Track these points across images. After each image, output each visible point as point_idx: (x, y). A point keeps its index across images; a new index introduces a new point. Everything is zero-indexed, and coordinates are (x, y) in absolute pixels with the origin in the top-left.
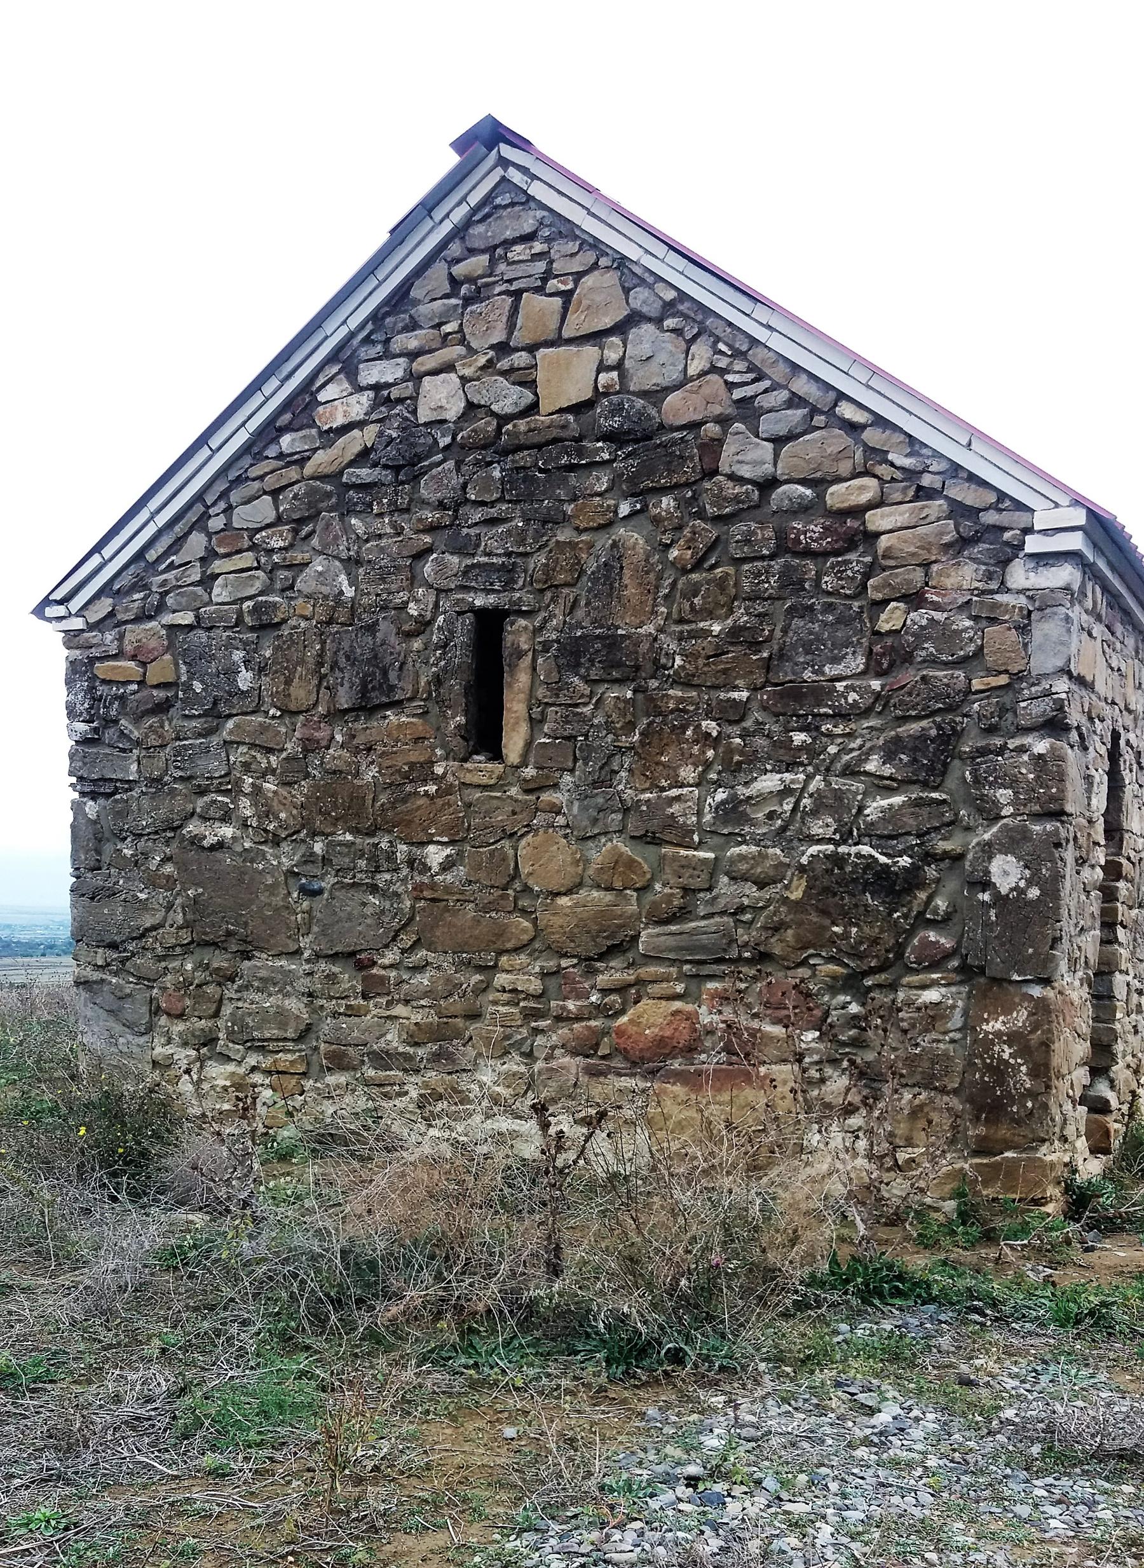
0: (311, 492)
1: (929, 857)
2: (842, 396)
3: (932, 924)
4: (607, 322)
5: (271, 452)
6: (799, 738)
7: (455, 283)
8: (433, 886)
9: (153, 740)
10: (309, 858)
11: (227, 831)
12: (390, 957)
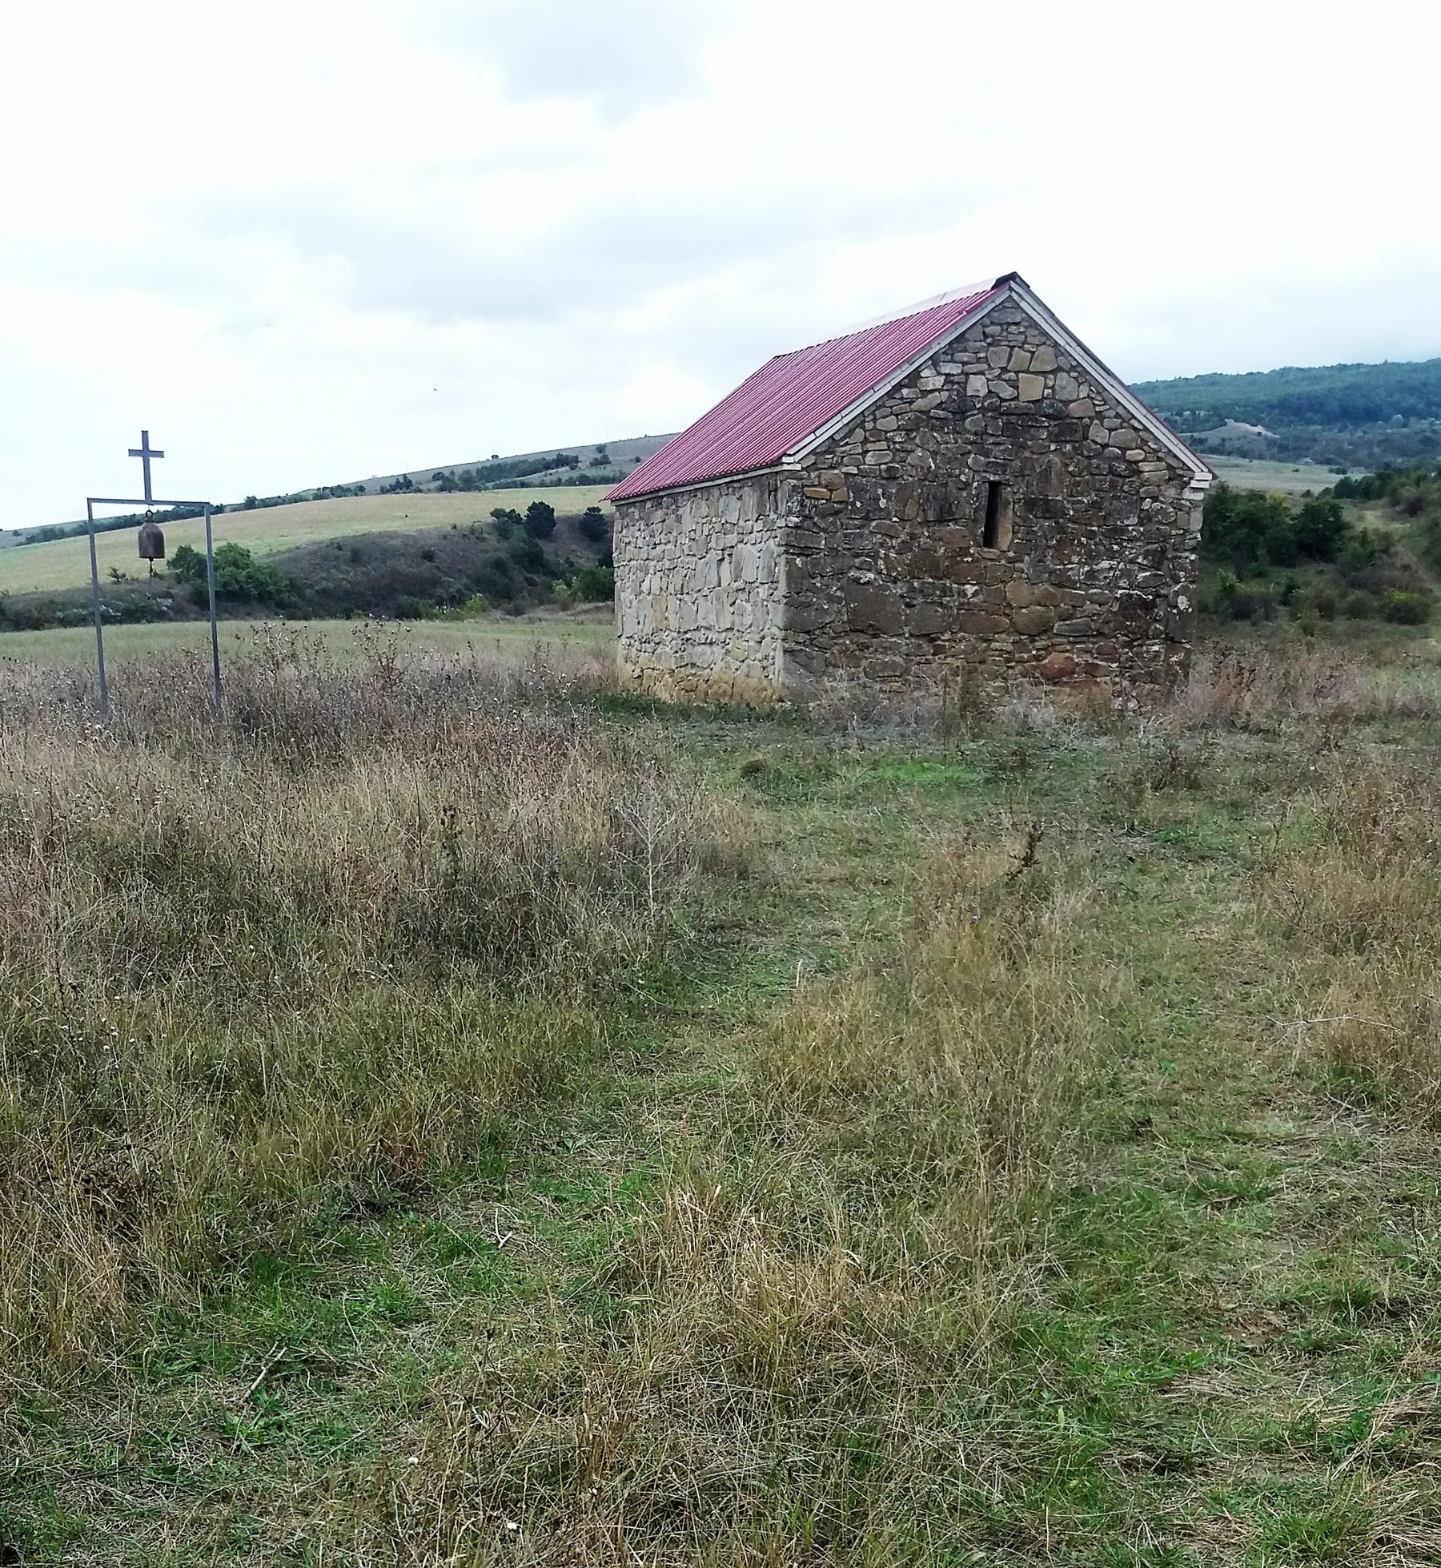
0: (917, 418)
1: (1158, 595)
2: (1134, 417)
3: (1156, 621)
4: (1048, 368)
5: (896, 396)
6: (1115, 547)
7: (986, 336)
8: (969, 604)
9: (832, 528)
10: (912, 589)
11: (871, 576)
12: (947, 636)
